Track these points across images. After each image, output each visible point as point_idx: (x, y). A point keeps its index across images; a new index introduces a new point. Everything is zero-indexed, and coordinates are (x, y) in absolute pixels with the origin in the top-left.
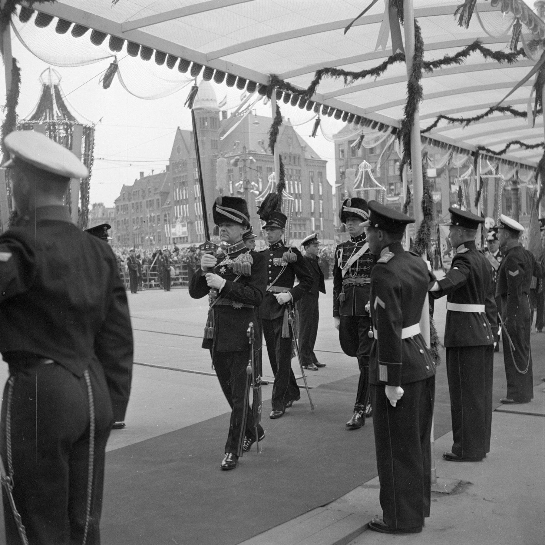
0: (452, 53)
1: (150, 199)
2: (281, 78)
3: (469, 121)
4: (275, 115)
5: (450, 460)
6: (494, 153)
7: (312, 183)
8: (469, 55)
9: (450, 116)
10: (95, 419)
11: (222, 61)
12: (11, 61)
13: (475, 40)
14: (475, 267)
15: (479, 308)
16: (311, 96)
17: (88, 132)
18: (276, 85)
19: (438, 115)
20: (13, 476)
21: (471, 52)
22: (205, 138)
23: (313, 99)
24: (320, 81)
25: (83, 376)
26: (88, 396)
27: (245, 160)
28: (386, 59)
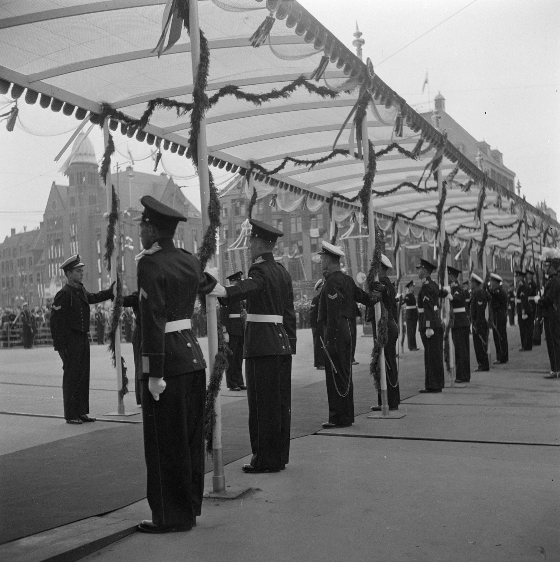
0: (279, 87)
1: (22, 257)
2: (113, 107)
3: (314, 163)
4: (108, 144)
5: (247, 472)
6: (347, 199)
7: (195, 242)
8: (295, 89)
9: (296, 158)
11: (42, 82)
13: (300, 76)
14: (271, 278)
15: (277, 319)
16: (144, 126)
19: (285, 157)
21: (297, 87)
22: (82, 194)
23: (146, 129)
24: (153, 112)
28: (217, 91)
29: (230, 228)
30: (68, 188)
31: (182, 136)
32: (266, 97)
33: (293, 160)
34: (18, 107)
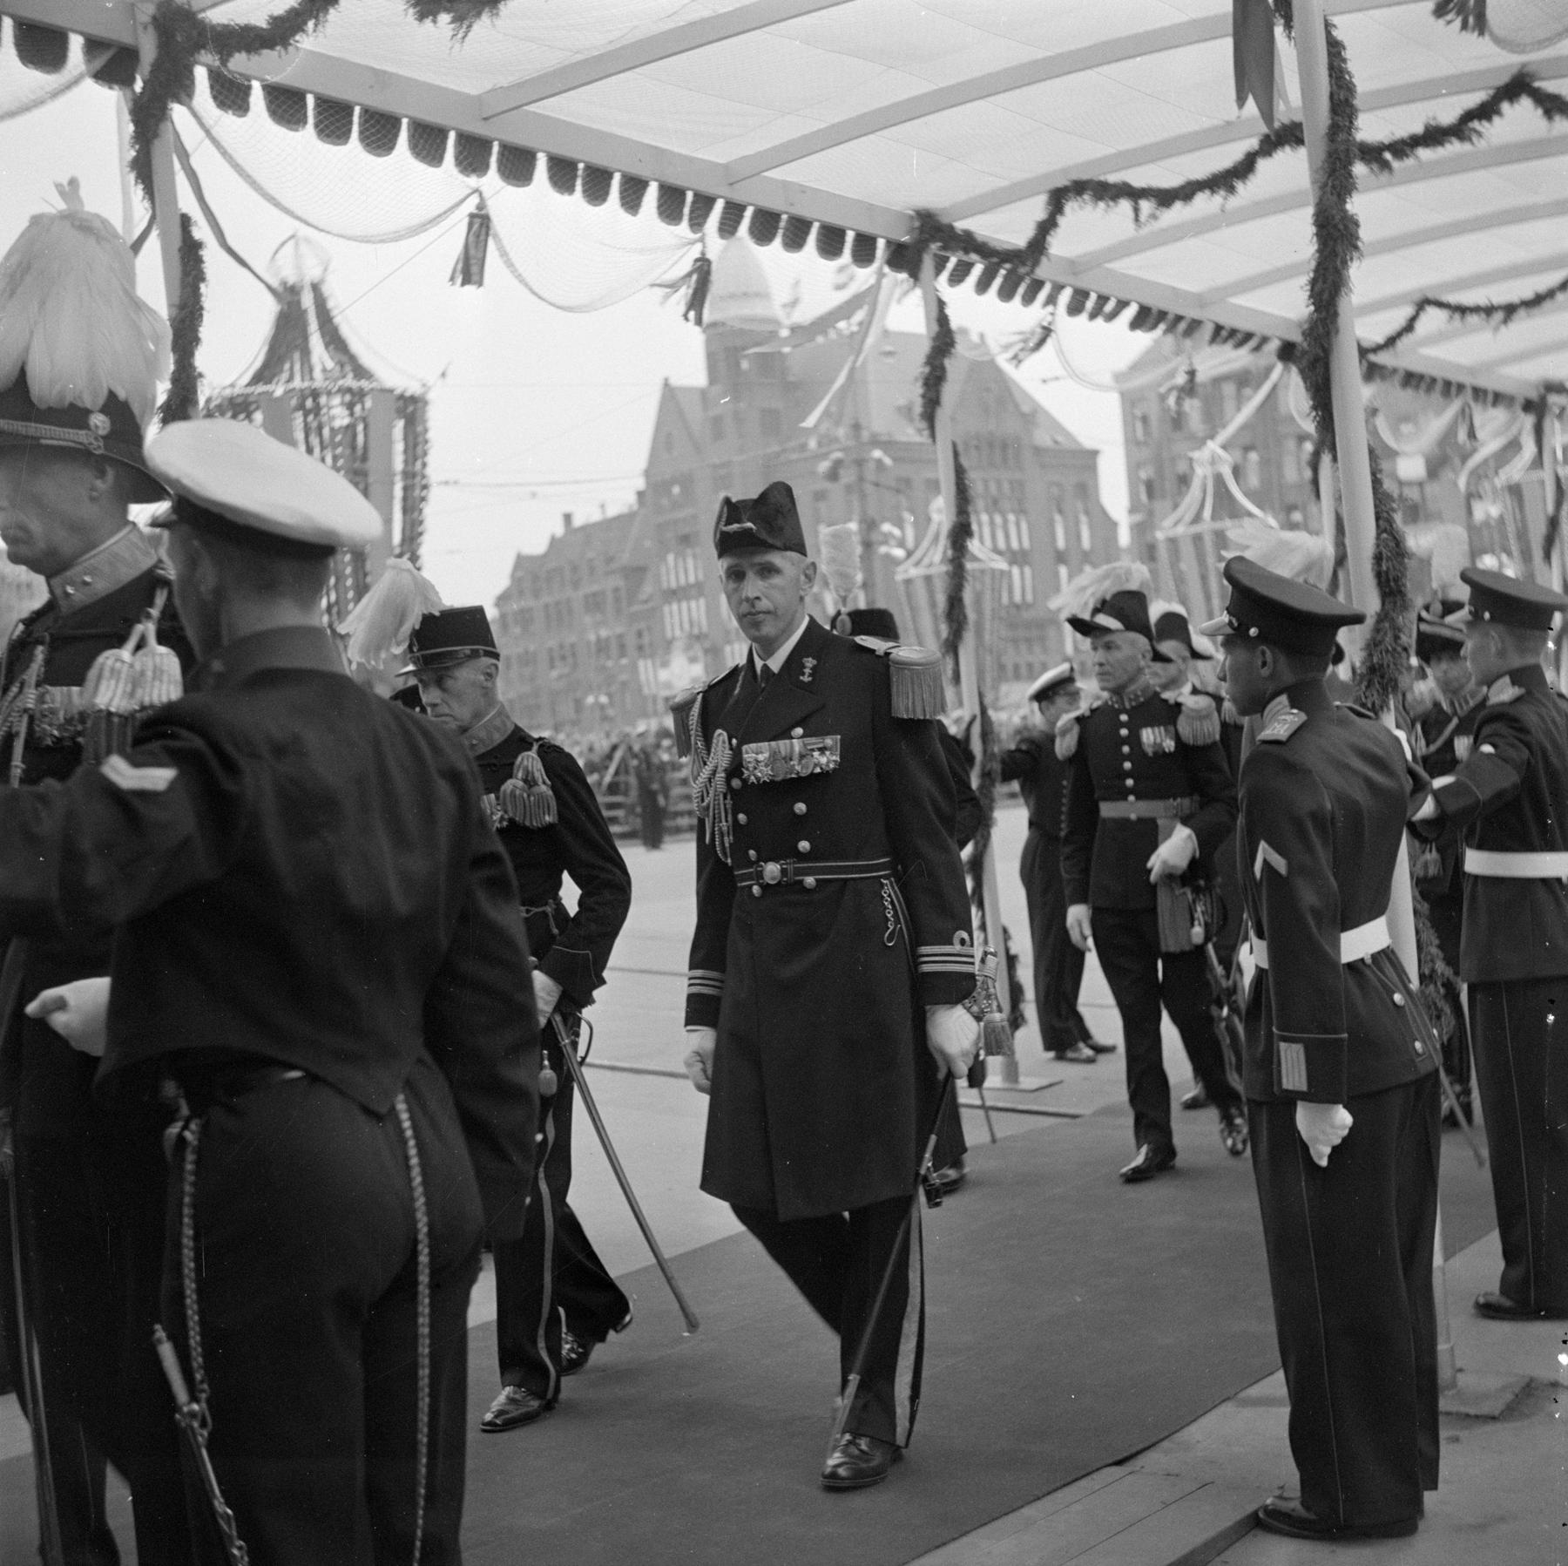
0: (1447, 112)
1: (595, 588)
2: (945, 220)
3: (1510, 310)
4: (935, 328)
5: (1493, 1318)
7: (1058, 518)
8: (1499, 113)
9: (1453, 298)
10: (430, 1234)
12: (177, 221)
13: (1514, 71)
16: (1036, 263)
17: (411, 409)
18: (933, 239)
19: (1418, 297)
20: (208, 1401)
21: (1505, 106)
23: (1041, 272)
24: (1061, 220)
25: (393, 1110)
26: (408, 1168)
27: (860, 463)
28: (1253, 143)
29: (1160, 470)
30: (703, 393)
31: (1133, 272)
32: (1403, 147)
33: (1440, 304)
34: (709, 256)
